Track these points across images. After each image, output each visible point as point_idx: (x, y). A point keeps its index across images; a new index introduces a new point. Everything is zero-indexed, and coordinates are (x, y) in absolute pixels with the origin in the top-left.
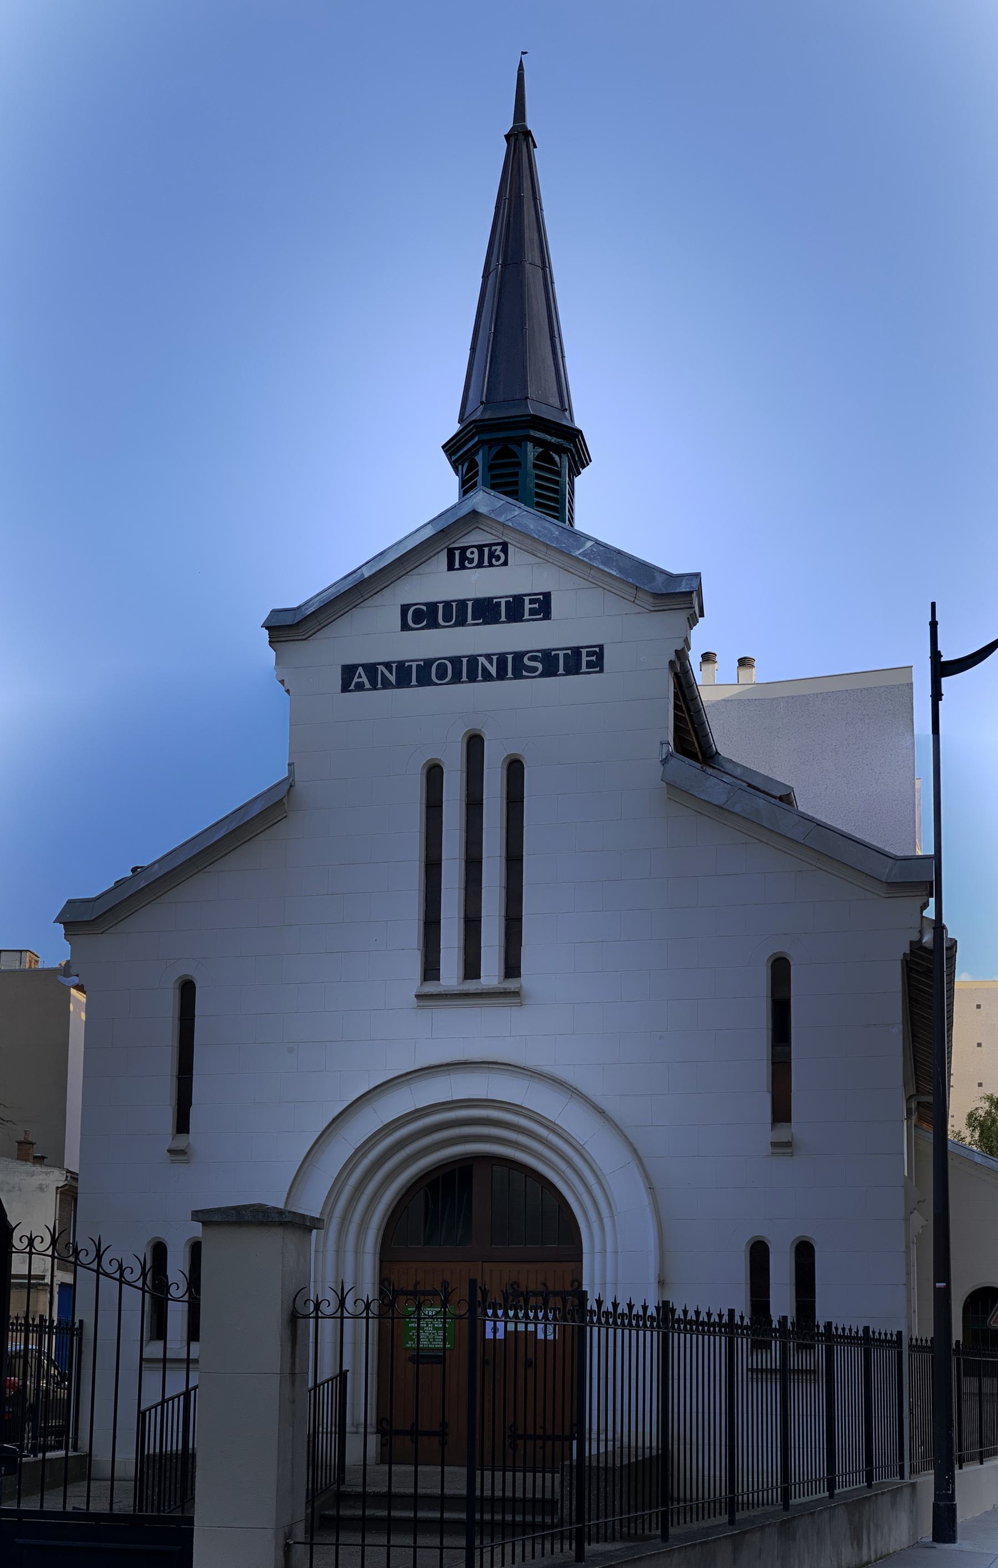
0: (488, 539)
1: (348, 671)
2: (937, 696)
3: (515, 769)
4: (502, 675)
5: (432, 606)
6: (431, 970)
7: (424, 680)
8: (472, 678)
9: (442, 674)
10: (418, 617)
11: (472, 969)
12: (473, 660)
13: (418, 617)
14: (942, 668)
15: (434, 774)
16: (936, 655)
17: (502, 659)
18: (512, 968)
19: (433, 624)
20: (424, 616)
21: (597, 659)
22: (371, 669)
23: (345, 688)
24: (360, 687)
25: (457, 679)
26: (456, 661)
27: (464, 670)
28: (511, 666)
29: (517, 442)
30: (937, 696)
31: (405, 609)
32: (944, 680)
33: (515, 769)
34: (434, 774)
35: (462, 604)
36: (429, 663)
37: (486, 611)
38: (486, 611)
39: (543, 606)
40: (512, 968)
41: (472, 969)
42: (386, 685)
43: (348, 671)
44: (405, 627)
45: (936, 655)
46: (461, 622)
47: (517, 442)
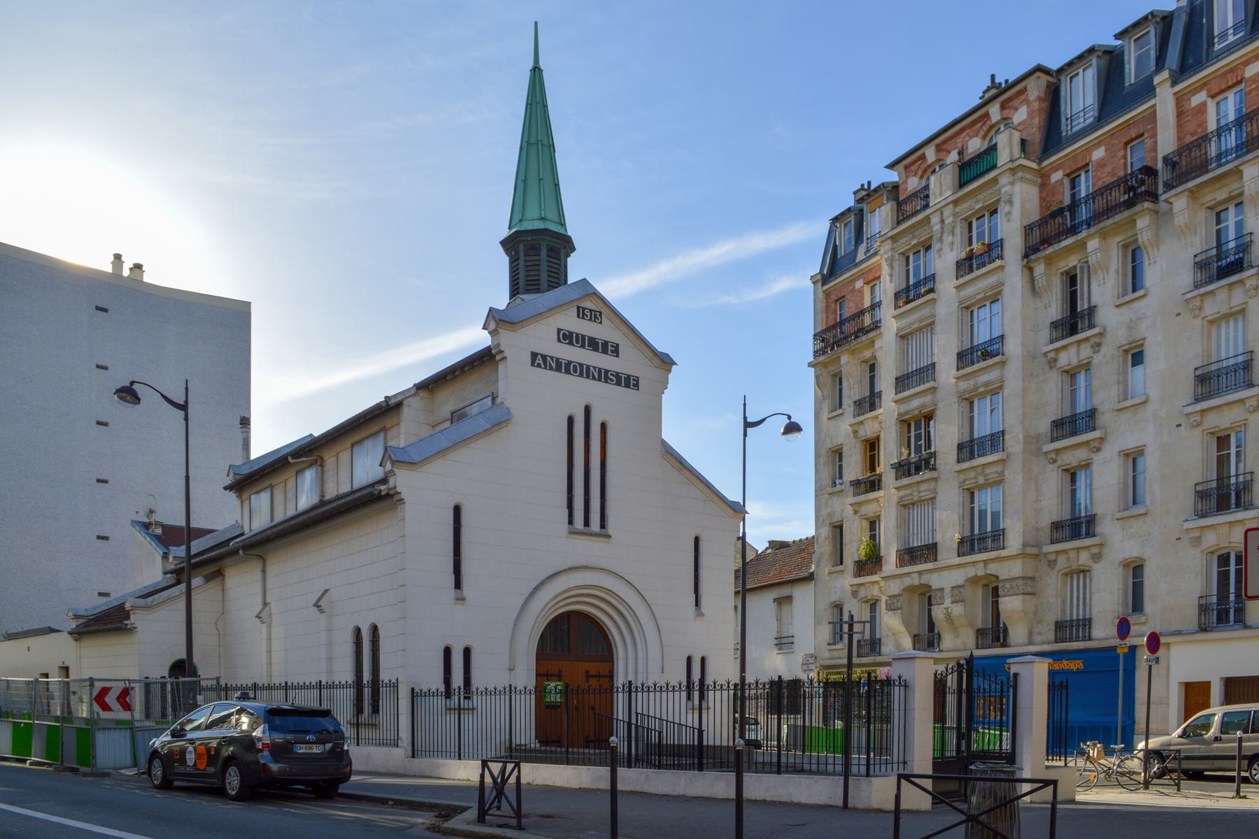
0: (594, 308)
1: (534, 355)
2: (745, 435)
3: (603, 427)
4: (600, 380)
5: (571, 333)
6: (571, 522)
7: (567, 372)
8: (588, 377)
9: (575, 371)
10: (565, 337)
11: (587, 523)
12: (588, 367)
13: (565, 337)
14: (748, 425)
15: (571, 420)
16: (745, 418)
17: (600, 370)
18: (603, 526)
19: (571, 343)
20: (567, 337)
21: (636, 386)
22: (544, 357)
23: (533, 364)
24: (539, 366)
25: (581, 375)
26: (581, 365)
27: (584, 371)
28: (604, 376)
29: (538, 255)
30: (745, 435)
31: (559, 330)
32: (749, 430)
33: (603, 427)
34: (571, 420)
35: (583, 336)
36: (570, 362)
37: (593, 344)
38: (593, 344)
39: (616, 351)
40: (603, 526)
41: (587, 523)
42: (551, 368)
43: (534, 355)
44: (559, 340)
45: (745, 418)
46: (583, 346)
47: (538, 255)
